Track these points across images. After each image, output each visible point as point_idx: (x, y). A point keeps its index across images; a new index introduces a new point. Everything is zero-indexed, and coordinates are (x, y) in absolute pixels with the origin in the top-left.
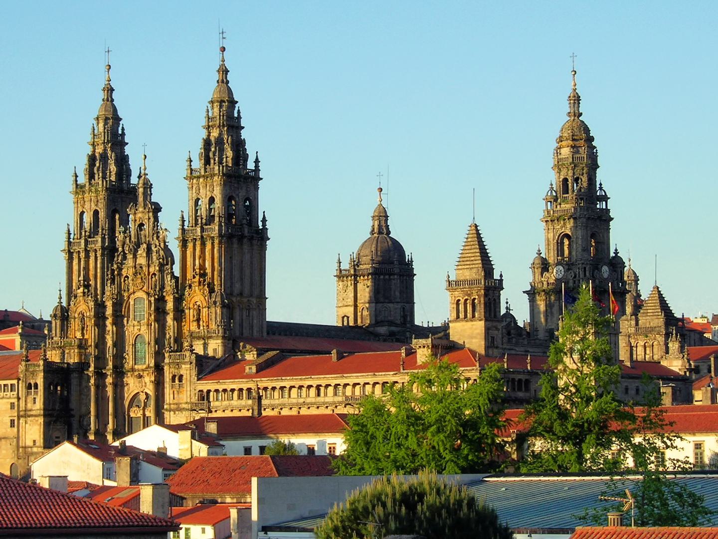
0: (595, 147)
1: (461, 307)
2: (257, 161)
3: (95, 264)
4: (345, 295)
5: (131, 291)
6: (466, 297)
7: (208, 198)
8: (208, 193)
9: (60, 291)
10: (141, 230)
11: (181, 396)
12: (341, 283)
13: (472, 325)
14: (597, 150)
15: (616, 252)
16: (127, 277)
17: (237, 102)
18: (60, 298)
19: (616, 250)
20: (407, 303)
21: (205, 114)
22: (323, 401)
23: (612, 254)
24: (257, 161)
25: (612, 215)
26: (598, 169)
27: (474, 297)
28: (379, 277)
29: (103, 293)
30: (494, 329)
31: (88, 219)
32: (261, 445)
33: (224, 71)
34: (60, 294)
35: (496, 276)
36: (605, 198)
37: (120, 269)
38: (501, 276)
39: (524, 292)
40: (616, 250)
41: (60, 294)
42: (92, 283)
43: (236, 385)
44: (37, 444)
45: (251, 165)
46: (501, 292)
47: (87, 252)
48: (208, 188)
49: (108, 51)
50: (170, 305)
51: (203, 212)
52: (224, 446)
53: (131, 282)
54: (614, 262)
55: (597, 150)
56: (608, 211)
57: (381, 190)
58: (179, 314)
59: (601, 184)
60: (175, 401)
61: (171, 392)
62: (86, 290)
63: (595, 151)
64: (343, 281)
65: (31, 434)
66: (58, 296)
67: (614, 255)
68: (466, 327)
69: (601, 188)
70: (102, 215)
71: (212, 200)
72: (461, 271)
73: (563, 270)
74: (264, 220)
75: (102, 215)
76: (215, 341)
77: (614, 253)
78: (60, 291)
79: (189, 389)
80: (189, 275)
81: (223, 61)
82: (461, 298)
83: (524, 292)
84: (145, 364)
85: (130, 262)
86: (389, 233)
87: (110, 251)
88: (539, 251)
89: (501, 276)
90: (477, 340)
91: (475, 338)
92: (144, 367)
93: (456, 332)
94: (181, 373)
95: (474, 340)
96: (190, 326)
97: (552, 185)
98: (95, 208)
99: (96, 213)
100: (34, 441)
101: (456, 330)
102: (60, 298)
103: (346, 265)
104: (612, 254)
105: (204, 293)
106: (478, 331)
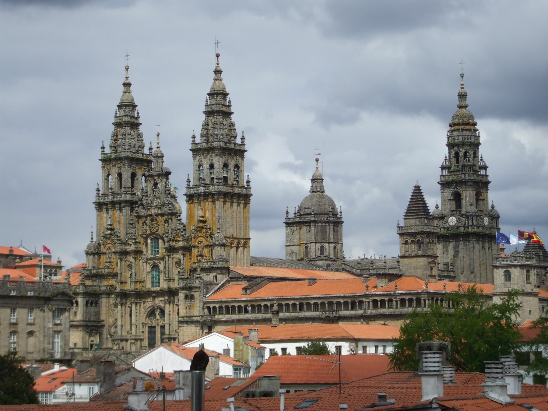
0: (478, 130)
2: (243, 138)
4: (292, 237)
5: (148, 232)
6: (413, 239)
7: (208, 165)
9: (92, 232)
10: (155, 188)
11: (192, 310)
12: (288, 228)
15: (493, 207)
16: (145, 222)
19: (493, 205)
21: (205, 103)
22: (304, 314)
23: (490, 208)
24: (243, 138)
26: (480, 146)
27: (419, 239)
30: (433, 262)
32: (283, 347)
34: (92, 235)
36: (485, 168)
40: (493, 205)
41: (92, 235)
42: (116, 226)
44: (78, 347)
45: (239, 141)
49: (127, 56)
51: (205, 174)
52: (265, 348)
54: (491, 213)
55: (479, 132)
56: (487, 176)
57: (317, 160)
59: (482, 157)
60: (188, 315)
61: (184, 307)
62: (113, 232)
63: (477, 132)
64: (290, 227)
65: (73, 339)
66: (90, 236)
67: (491, 209)
69: (481, 160)
72: (408, 220)
73: (455, 220)
74: (248, 182)
78: (92, 232)
79: (198, 306)
81: (218, 64)
82: (408, 240)
84: (159, 286)
86: (323, 192)
88: (437, 205)
90: (421, 270)
91: (419, 268)
92: (158, 289)
93: (405, 264)
94: (192, 293)
95: (418, 271)
97: (446, 157)
100: (75, 344)
101: (404, 263)
102: (92, 238)
103: (291, 215)
104: (490, 208)
106: (421, 264)
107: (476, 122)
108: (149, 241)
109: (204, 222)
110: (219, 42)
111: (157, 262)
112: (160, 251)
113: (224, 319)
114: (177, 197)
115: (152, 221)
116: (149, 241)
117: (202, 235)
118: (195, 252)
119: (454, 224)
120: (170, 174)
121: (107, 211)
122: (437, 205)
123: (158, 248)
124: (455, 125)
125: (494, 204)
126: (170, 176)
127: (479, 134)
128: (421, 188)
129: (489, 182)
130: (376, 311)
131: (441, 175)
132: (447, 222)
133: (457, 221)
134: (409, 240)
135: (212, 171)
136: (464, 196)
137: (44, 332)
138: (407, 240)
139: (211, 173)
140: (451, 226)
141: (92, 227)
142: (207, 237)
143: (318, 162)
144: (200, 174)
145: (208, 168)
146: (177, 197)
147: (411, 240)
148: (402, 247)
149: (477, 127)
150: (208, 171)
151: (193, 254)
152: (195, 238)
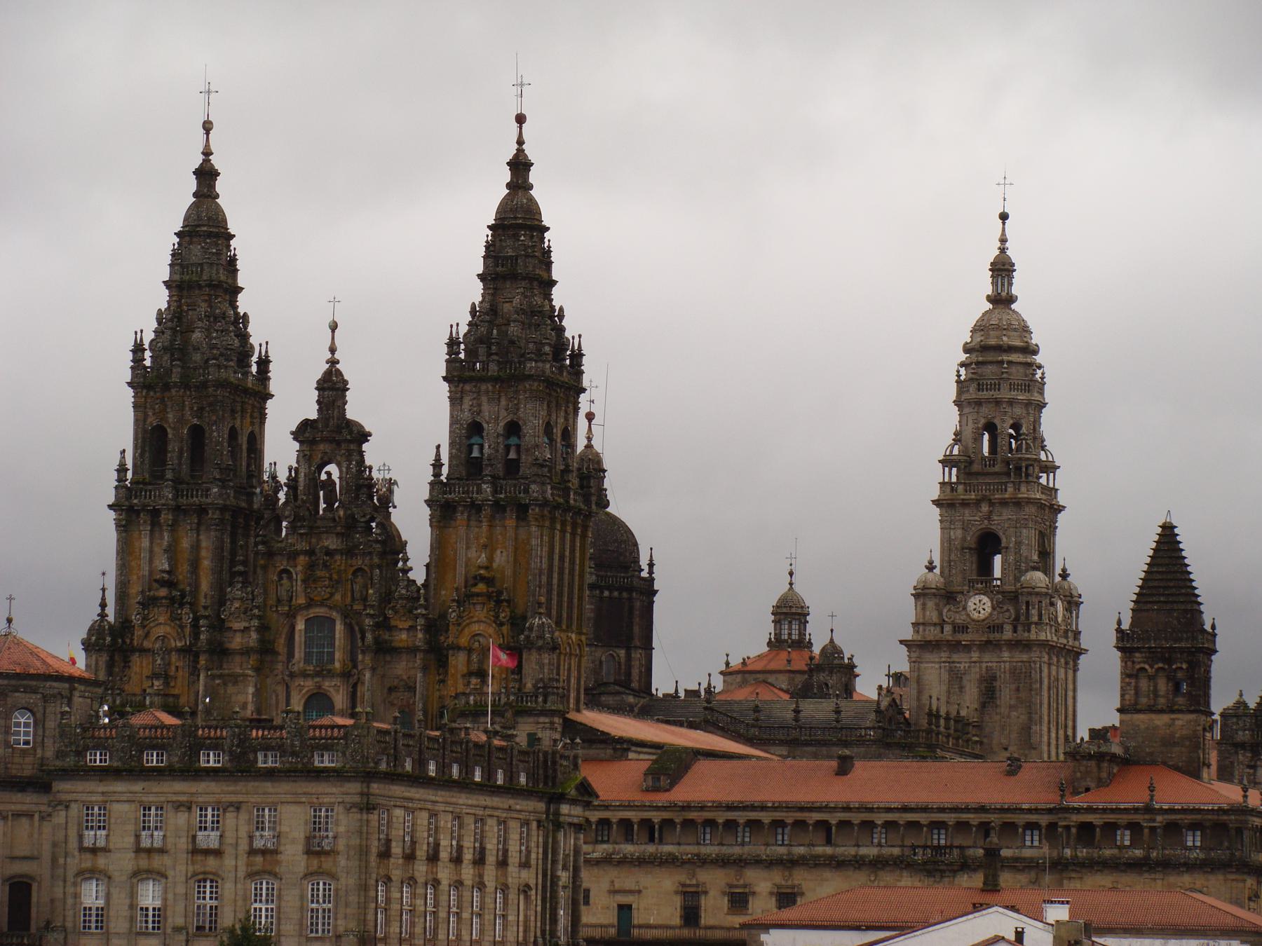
0: (1040, 367)
6: (1161, 665)
7: (502, 424)
8: (503, 413)
9: (104, 590)
13: (1173, 719)
14: (1043, 374)
17: (548, 229)
18: (103, 605)
19: (1064, 570)
20: (645, 649)
25: (1062, 499)
28: (602, 592)
29: (221, 601)
34: (103, 599)
35: (1208, 627)
38: (1213, 627)
39: (901, 642)
40: (1064, 570)
41: (103, 599)
43: (634, 813)
46: (1213, 657)
48: (503, 402)
53: (299, 587)
55: (1043, 374)
68: (1158, 723)
76: (531, 720)
77: (1060, 575)
78: (104, 590)
81: (520, 142)
82: (1147, 667)
83: (901, 642)
88: (931, 562)
89: (1213, 627)
98: (195, 421)
102: (103, 605)
105: (497, 617)
107: (1037, 345)
108: (300, 626)
109: (489, 581)
110: (525, 81)
111: (327, 684)
112: (338, 655)
113: (595, 855)
114: (395, 507)
115: (311, 567)
116: (300, 626)
117: (484, 619)
118: (458, 662)
119: (982, 616)
120: (368, 441)
121: (152, 531)
122: (931, 562)
123: (333, 645)
124: (984, 348)
125: (1067, 567)
126: (365, 447)
127: (1042, 378)
128: (1176, 531)
129: (1060, 509)
130: (1087, 853)
131: (942, 481)
132: (965, 608)
133: (993, 608)
134: (1152, 667)
135: (513, 440)
137: (544, 887)
138: (1142, 665)
139: (508, 448)
140: (974, 620)
141: (104, 574)
142: (502, 624)
143: (593, 422)
144: (470, 447)
145: (500, 429)
146: (395, 507)
147: (1156, 666)
148: (1129, 684)
149: (1039, 359)
150: (500, 440)
151: (451, 670)
152: (459, 625)
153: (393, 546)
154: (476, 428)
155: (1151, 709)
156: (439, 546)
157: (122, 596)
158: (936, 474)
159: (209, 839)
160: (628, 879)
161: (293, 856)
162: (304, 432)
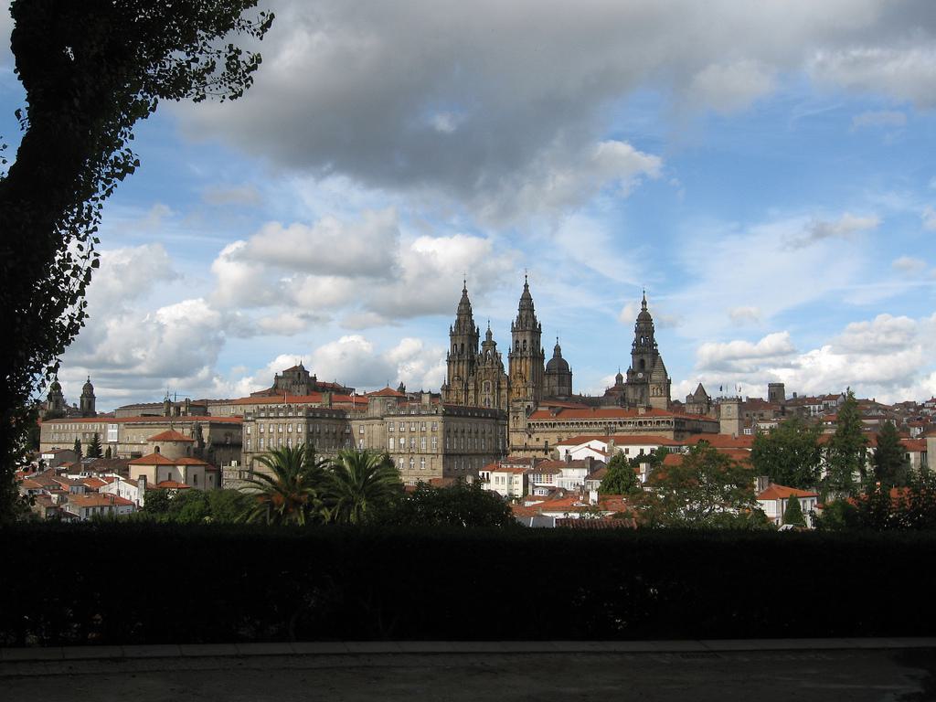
1: (655, 391)
3: (464, 367)
31: (459, 347)
33: (526, 286)
37: (477, 369)
42: (461, 374)
47: (459, 361)
50: (504, 385)
58: (510, 390)
70: (466, 345)
71: (525, 341)
74: (543, 350)
75: (466, 345)
80: (514, 373)
85: (481, 367)
87: (472, 362)
96: (514, 396)
99: (463, 345)
136: (646, 361)
153: (501, 367)
154: (517, 342)
155: (657, 396)
156: (510, 367)
157: (449, 380)
158: (631, 347)
159: (413, 429)
160: (547, 435)
161: (429, 432)
162: (484, 343)
